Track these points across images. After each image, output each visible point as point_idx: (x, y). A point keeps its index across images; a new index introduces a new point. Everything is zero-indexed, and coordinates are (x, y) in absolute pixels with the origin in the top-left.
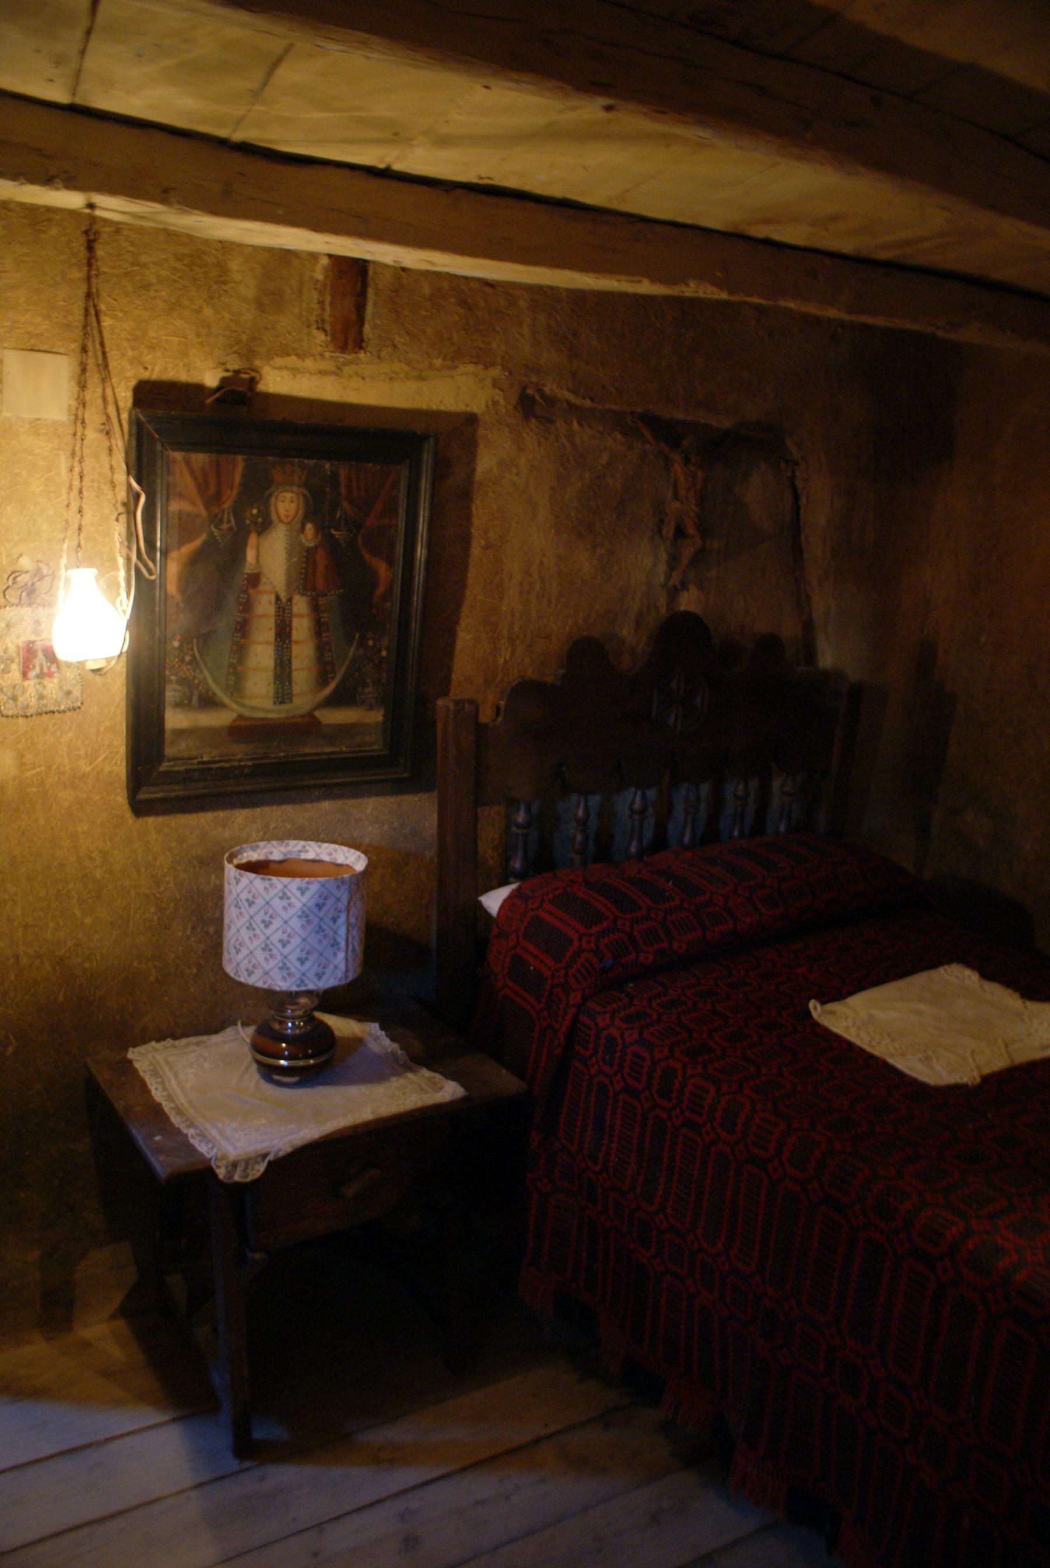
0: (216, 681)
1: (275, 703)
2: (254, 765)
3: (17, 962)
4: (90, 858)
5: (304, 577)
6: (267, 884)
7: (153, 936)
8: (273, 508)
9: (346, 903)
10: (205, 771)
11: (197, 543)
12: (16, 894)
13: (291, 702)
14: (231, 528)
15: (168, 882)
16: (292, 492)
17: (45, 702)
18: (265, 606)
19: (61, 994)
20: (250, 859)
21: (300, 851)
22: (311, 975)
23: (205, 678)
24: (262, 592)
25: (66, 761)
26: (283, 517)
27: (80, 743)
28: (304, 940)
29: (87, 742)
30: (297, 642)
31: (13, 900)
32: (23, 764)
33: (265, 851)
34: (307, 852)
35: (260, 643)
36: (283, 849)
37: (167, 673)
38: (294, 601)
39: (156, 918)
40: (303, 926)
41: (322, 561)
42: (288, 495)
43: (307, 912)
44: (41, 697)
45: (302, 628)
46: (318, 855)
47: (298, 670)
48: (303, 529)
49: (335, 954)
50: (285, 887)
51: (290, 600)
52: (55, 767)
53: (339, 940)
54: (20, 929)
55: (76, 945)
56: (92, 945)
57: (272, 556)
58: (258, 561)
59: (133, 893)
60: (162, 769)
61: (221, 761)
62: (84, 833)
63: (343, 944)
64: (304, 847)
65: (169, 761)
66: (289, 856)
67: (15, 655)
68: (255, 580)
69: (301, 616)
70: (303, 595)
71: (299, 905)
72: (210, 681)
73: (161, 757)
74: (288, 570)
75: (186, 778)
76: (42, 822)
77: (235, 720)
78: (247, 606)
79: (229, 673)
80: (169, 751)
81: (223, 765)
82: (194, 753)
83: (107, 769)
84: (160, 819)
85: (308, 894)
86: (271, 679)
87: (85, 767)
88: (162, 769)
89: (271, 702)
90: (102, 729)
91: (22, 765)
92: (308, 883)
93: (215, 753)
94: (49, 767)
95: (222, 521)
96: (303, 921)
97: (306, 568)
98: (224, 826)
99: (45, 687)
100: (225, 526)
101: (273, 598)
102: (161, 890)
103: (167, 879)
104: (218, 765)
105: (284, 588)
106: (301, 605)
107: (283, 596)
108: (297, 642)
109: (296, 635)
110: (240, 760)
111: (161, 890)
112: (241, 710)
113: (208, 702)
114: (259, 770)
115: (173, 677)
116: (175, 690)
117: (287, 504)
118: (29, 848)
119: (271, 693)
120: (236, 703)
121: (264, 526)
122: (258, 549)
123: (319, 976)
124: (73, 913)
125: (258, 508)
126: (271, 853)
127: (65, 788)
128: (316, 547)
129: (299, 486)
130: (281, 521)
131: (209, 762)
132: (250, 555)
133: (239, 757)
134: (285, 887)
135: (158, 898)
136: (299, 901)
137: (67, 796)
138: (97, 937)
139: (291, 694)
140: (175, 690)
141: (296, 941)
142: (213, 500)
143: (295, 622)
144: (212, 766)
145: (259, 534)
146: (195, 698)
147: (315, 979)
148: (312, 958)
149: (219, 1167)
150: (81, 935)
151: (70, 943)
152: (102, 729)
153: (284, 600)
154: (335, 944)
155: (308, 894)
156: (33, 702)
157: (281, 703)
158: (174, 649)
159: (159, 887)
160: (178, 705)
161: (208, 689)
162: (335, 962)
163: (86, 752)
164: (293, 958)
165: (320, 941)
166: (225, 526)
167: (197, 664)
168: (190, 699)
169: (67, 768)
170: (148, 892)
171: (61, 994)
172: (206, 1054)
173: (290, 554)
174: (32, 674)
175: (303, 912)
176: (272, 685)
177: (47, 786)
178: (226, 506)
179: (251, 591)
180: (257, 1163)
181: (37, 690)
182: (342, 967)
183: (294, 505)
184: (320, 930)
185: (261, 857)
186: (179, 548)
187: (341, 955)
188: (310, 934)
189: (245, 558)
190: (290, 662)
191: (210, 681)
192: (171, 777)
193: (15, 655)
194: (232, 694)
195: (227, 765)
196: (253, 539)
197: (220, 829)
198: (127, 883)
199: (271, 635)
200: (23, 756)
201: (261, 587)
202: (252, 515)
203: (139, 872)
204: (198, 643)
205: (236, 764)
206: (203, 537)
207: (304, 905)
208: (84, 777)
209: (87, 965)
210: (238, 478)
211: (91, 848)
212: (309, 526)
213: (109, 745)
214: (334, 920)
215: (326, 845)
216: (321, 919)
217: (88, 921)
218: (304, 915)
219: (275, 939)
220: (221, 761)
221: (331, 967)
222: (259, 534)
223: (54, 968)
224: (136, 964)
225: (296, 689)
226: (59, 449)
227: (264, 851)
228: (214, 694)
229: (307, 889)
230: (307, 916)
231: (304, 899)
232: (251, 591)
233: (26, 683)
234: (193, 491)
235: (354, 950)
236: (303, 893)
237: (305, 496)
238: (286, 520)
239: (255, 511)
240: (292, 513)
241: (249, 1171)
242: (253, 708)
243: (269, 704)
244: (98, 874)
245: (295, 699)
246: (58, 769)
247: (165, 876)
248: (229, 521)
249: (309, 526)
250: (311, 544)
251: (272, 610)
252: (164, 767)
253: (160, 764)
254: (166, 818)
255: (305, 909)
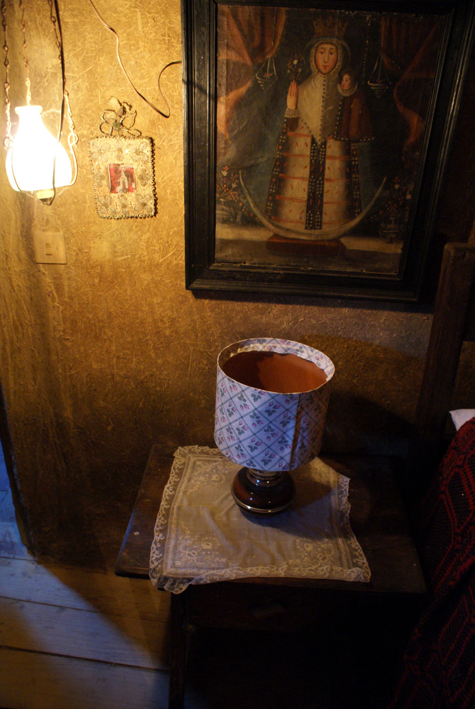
0: (256, 205)
1: (306, 228)
2: (285, 274)
3: (113, 378)
4: (162, 321)
5: (339, 121)
6: (231, 384)
7: (205, 379)
8: (312, 59)
9: (295, 413)
10: (245, 274)
11: (243, 90)
12: (111, 336)
13: (320, 229)
14: (273, 77)
15: (217, 346)
16: (332, 44)
17: (127, 210)
18: (302, 147)
19: (141, 403)
20: (256, 349)
21: (298, 350)
22: (259, 459)
23: (248, 202)
24: (300, 135)
25: (145, 253)
26: (322, 68)
27: (155, 241)
28: (254, 434)
29: (160, 241)
30: (329, 180)
31: (110, 340)
32: (116, 252)
33: (271, 345)
34: (302, 352)
35: (297, 178)
36: (285, 346)
37: (217, 195)
38: (328, 145)
39: (207, 368)
40: (254, 424)
41: (356, 108)
42: (328, 47)
43: (258, 415)
44: (124, 206)
45: (333, 168)
46: (309, 357)
47: (327, 203)
48: (340, 80)
49: (282, 449)
50: (243, 391)
51: (325, 143)
52: (137, 256)
53: (287, 439)
54: (115, 359)
55: (151, 375)
56: (162, 377)
57: (310, 104)
58: (296, 107)
59: (192, 348)
60: (211, 268)
61: (258, 268)
62: (158, 304)
63: (290, 443)
64: (301, 347)
65: (219, 262)
66: (289, 352)
67: (105, 175)
68: (293, 123)
69: (333, 158)
70: (336, 139)
71: (252, 408)
72: (252, 205)
73: (212, 259)
74: (324, 116)
75: (230, 276)
76: (129, 292)
77: (271, 238)
78: (286, 146)
79: (268, 199)
80: (218, 255)
81: (259, 270)
82: (238, 259)
83: (174, 262)
84: (214, 302)
85: (259, 402)
86: (304, 208)
87: (158, 258)
88: (211, 268)
89: (304, 227)
90: (171, 233)
91: (114, 253)
92: (260, 392)
93: (256, 260)
94: (134, 256)
95: (265, 70)
96: (255, 421)
97: (341, 116)
98: (262, 314)
99: (126, 199)
100: (268, 75)
101: (309, 140)
102: (212, 350)
103: (217, 344)
104: (256, 270)
105: (319, 132)
106: (334, 148)
107: (318, 138)
108: (329, 180)
109: (327, 174)
110: (274, 269)
111: (212, 350)
112: (277, 231)
113: (250, 221)
114: (288, 279)
115: (221, 200)
116: (223, 210)
117: (326, 55)
118: (121, 308)
119: (304, 220)
120: (273, 224)
121: (304, 76)
122: (297, 97)
123: (266, 462)
124: (150, 355)
125: (299, 60)
126: (275, 347)
127: (145, 271)
128: (351, 97)
129: (338, 38)
130: (319, 71)
131: (248, 267)
132: (290, 102)
133: (275, 266)
134: (243, 391)
135: (210, 356)
136: (252, 405)
137: (146, 277)
138: (166, 372)
139: (321, 222)
140: (223, 210)
141: (248, 433)
142: (257, 51)
143: (328, 163)
144: (251, 270)
145: (299, 83)
146: (239, 218)
147: (262, 464)
148: (260, 448)
149: (154, 577)
150: (155, 370)
151: (147, 373)
152: (171, 233)
153: (319, 143)
154: (283, 441)
155: (259, 402)
156: (119, 209)
157: (311, 228)
158: (224, 177)
159: (210, 348)
160: (224, 221)
161: (250, 211)
162: (282, 454)
163: (160, 248)
164: (246, 444)
165: (268, 438)
166: (268, 75)
167: (242, 192)
168: (235, 218)
169: (146, 258)
170: (202, 350)
171: (141, 403)
172: (220, 468)
173: (326, 102)
174: (119, 188)
175: (255, 414)
176: (304, 214)
177: (132, 269)
178: (269, 56)
179: (290, 133)
180: (184, 583)
181: (121, 202)
182: (288, 458)
183: (333, 57)
184: (269, 429)
185: (266, 350)
186: (227, 94)
187: (288, 451)
188: (261, 430)
189: (285, 104)
190: (322, 196)
191: (252, 205)
192: (219, 275)
193: (105, 175)
194: (270, 217)
195: (263, 271)
196: (293, 88)
197: (260, 316)
198: (188, 342)
199: (306, 172)
200: (115, 246)
201: (299, 131)
202: (294, 66)
203: (196, 336)
204: (243, 174)
205: (271, 271)
206: (249, 84)
207: (256, 409)
208: (158, 266)
209: (158, 389)
210: (281, 30)
211: (163, 315)
212: (346, 77)
213: (176, 245)
214: (284, 424)
215: (317, 351)
216: (271, 422)
217: (160, 361)
218: (254, 416)
219: (235, 425)
220: (258, 268)
221: (278, 457)
222: (299, 83)
223: (137, 386)
224: (191, 394)
225: (325, 219)
226: (136, 7)
227: (270, 345)
228: (255, 216)
229: (259, 397)
230: (258, 418)
231: (257, 404)
232: (290, 133)
233: (113, 195)
234: (239, 41)
235: (303, 446)
236: (255, 400)
237: (344, 48)
238: (324, 71)
239: (295, 62)
240: (330, 64)
241: (175, 586)
242: (288, 230)
243: (301, 228)
244: (167, 332)
245: (324, 226)
246: (140, 258)
247: (215, 342)
248: (271, 71)
249: (346, 77)
250: (347, 95)
251: (307, 151)
252: (214, 266)
253: (210, 265)
254: (218, 302)
255: (256, 411)
